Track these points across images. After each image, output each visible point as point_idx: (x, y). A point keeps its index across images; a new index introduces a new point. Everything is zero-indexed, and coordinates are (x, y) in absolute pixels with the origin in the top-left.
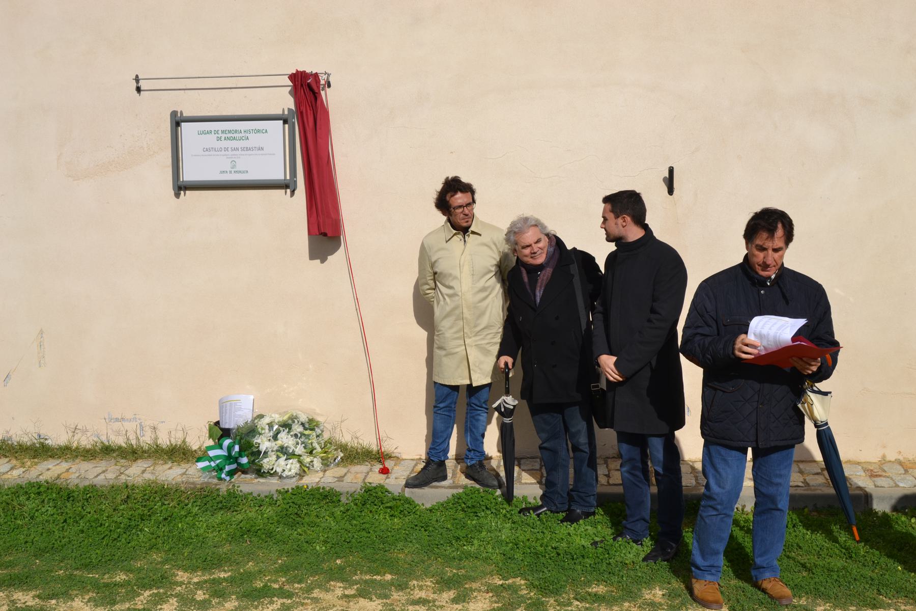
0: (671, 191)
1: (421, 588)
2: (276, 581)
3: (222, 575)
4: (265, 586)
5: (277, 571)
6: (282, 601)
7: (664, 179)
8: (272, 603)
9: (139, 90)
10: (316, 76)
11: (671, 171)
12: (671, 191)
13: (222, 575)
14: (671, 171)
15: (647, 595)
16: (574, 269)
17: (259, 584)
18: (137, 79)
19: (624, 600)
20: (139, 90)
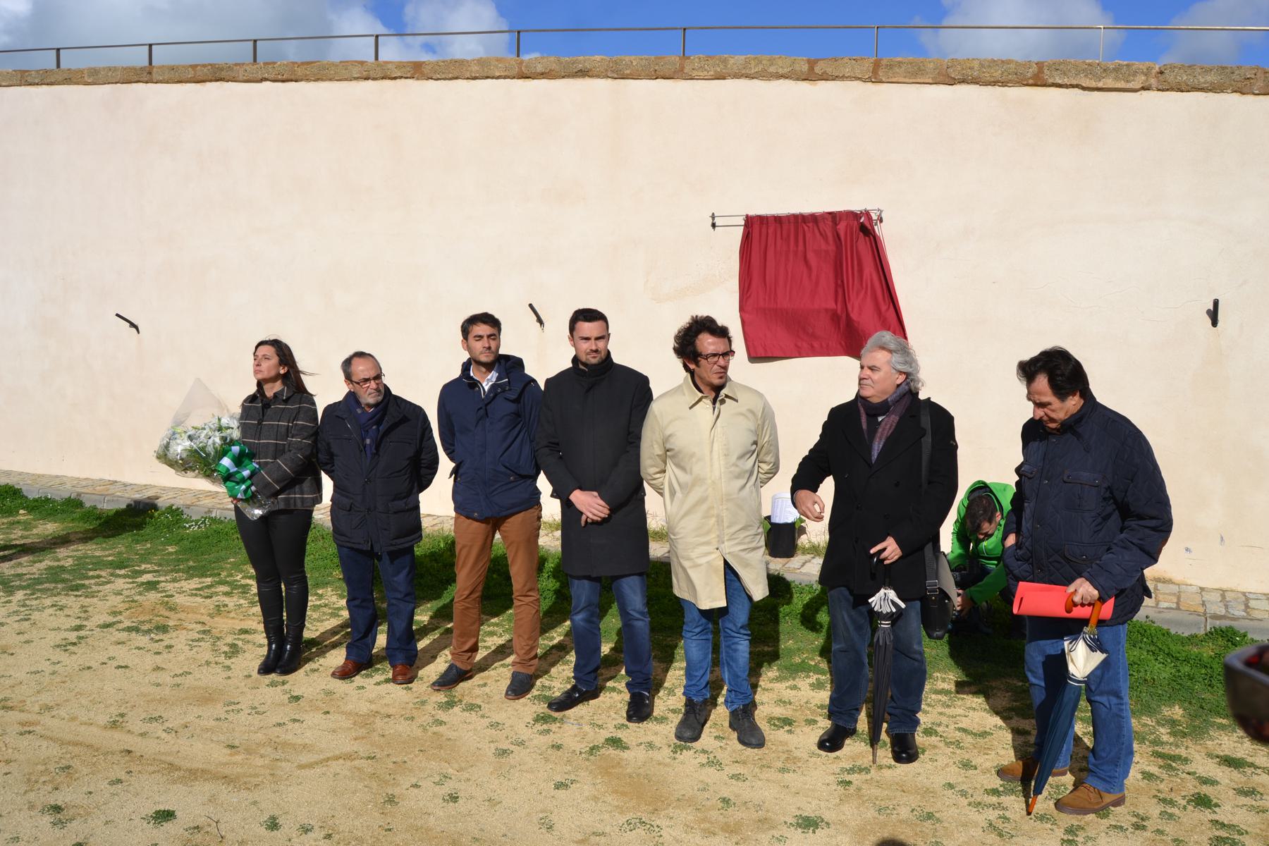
0: (1215, 323)
1: (944, 680)
2: (813, 659)
3: (766, 649)
4: (803, 661)
5: (813, 651)
6: (816, 676)
7: (1208, 312)
8: (808, 677)
9: (714, 225)
10: (867, 214)
11: (1216, 303)
12: (1215, 323)
13: (766, 649)
14: (1216, 303)
15: (1166, 712)
16: (926, 421)
17: (797, 660)
18: (713, 217)
19: (1142, 714)
20: (714, 225)
